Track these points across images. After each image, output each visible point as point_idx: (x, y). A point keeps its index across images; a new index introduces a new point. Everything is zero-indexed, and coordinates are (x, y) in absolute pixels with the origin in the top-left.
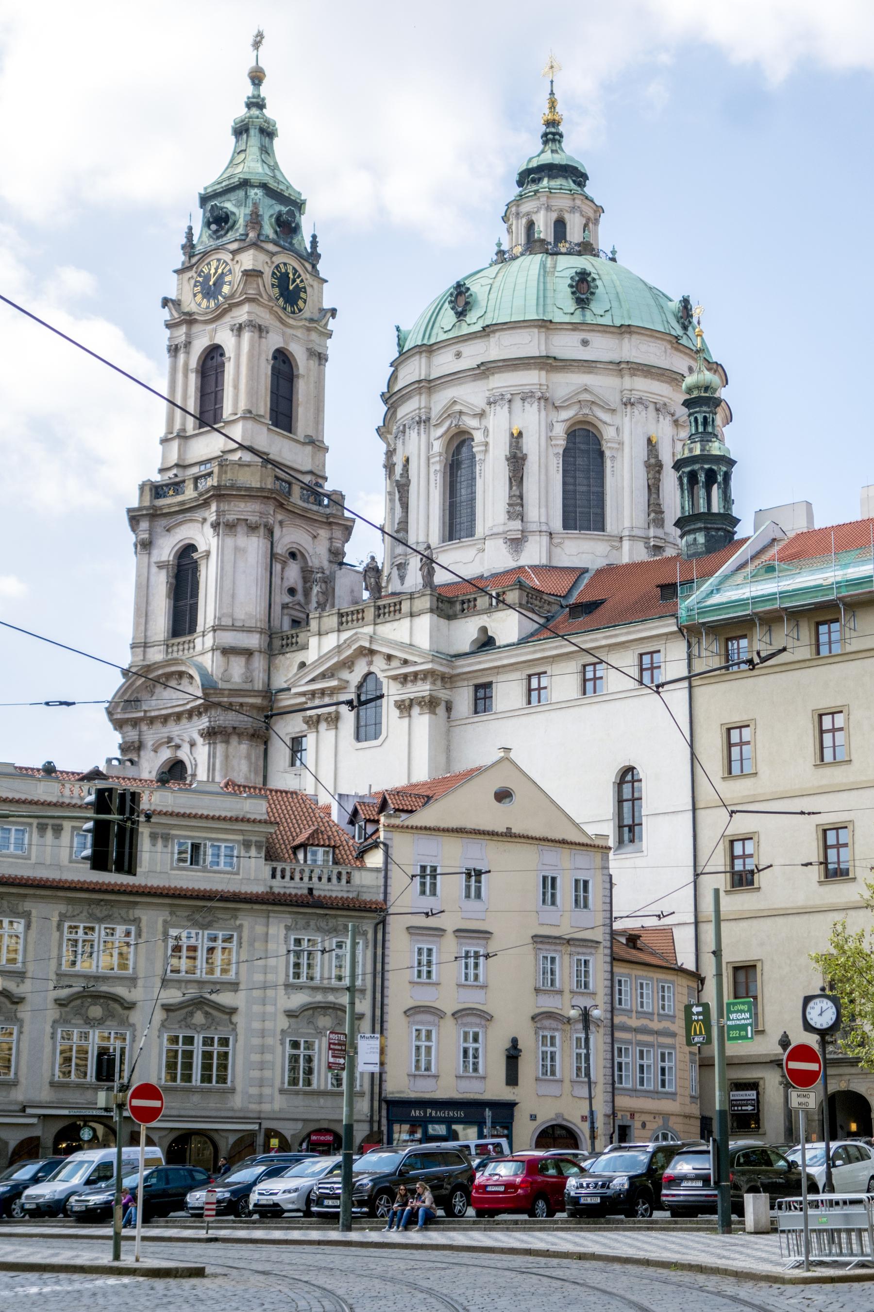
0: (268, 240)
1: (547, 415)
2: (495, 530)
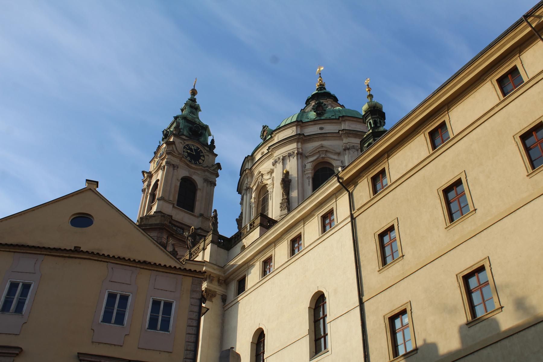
1: (302, 162)
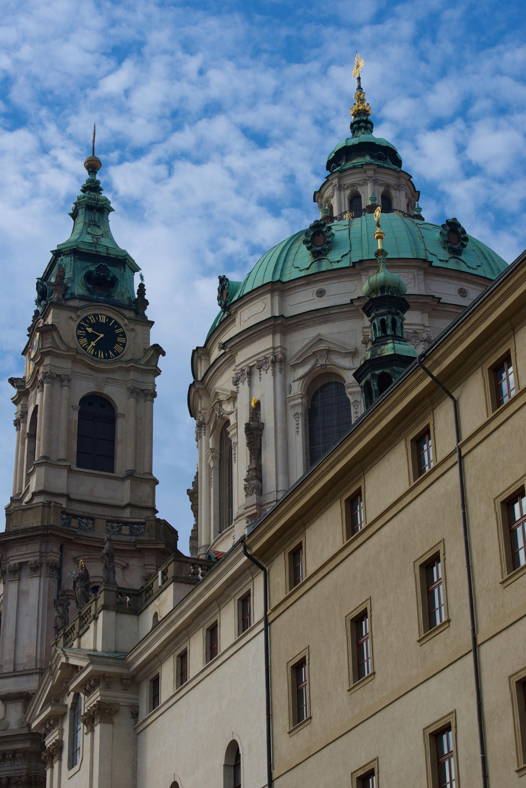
0: (73, 297)
1: (285, 378)
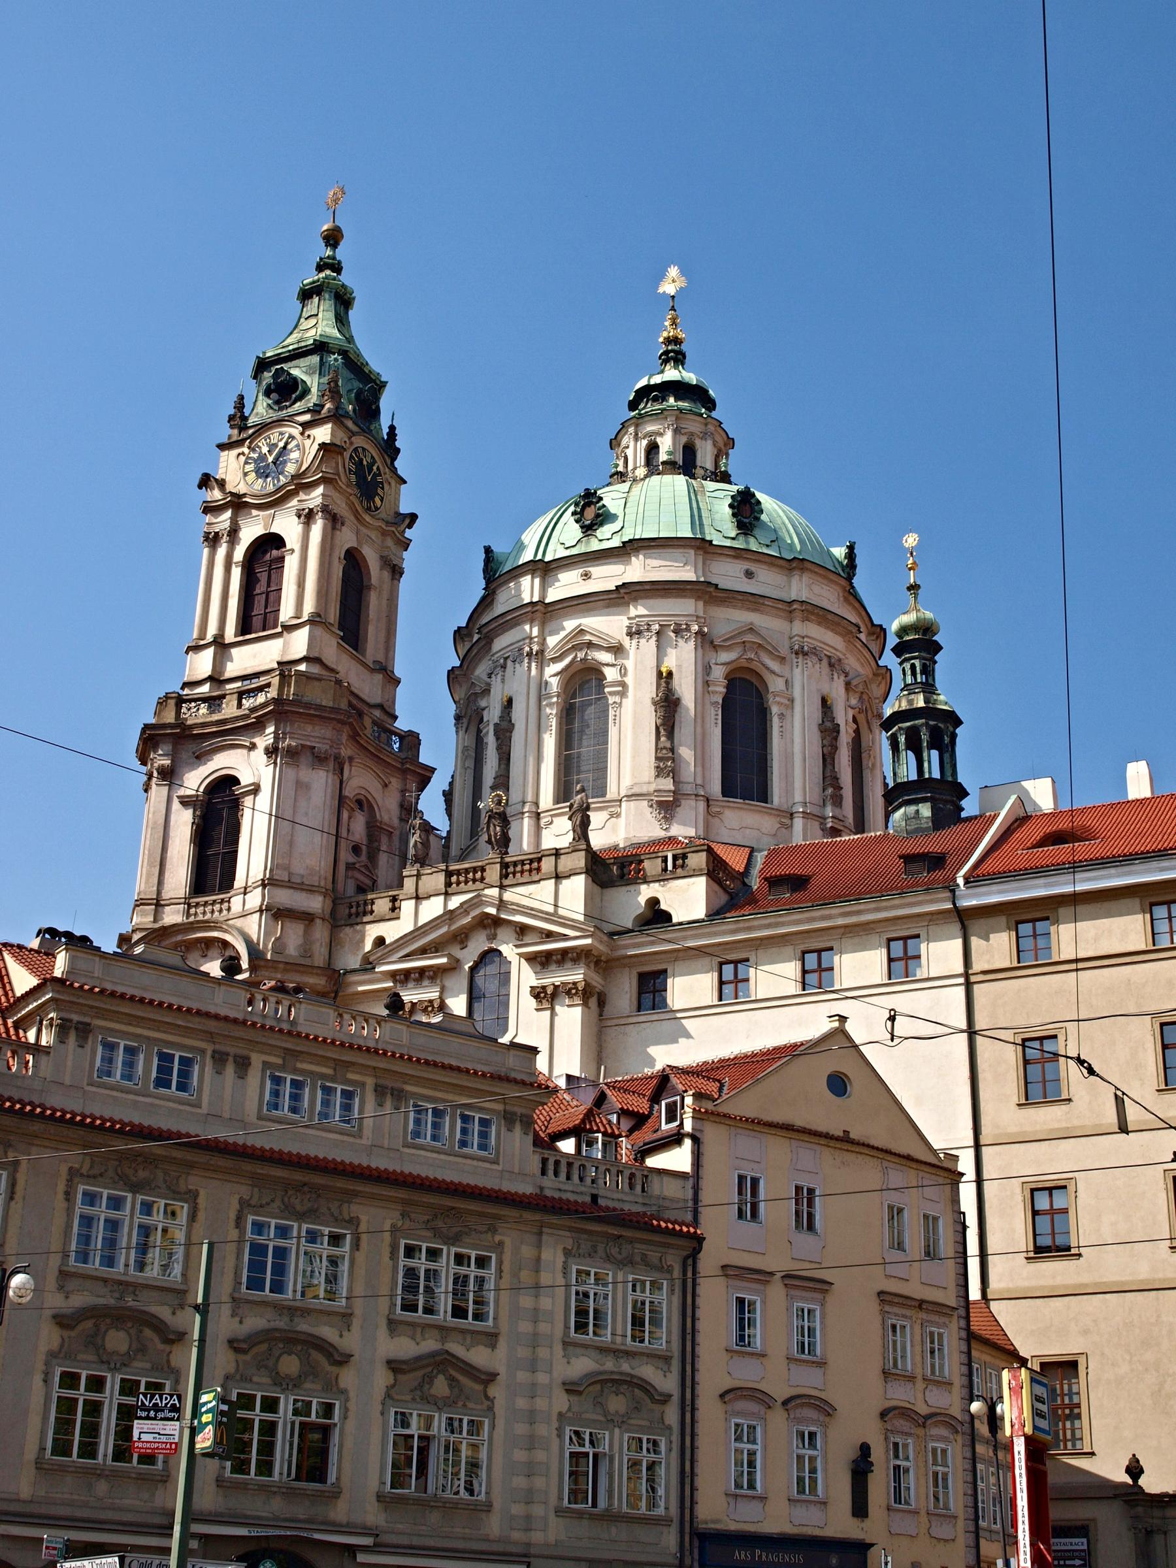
0: (346, 415)
2: (636, 790)
